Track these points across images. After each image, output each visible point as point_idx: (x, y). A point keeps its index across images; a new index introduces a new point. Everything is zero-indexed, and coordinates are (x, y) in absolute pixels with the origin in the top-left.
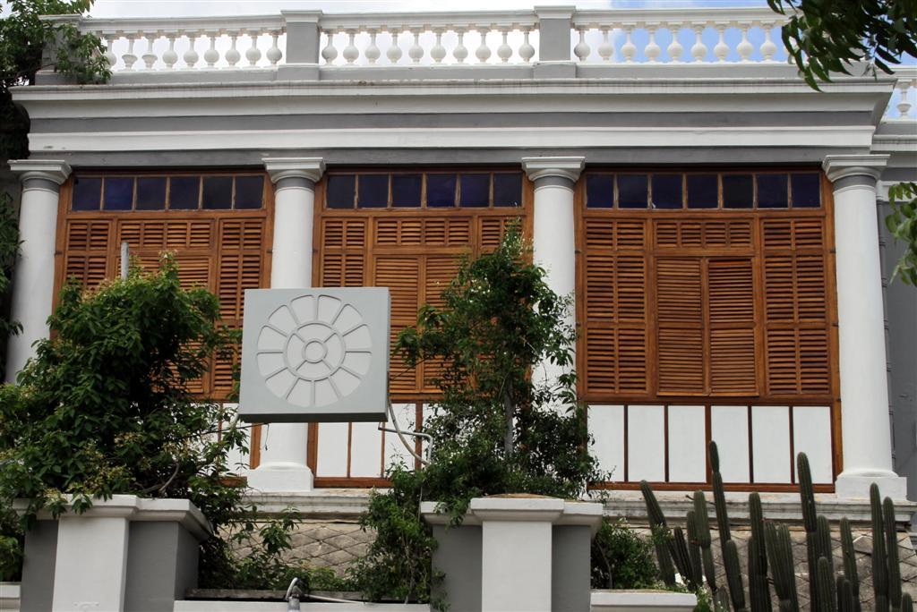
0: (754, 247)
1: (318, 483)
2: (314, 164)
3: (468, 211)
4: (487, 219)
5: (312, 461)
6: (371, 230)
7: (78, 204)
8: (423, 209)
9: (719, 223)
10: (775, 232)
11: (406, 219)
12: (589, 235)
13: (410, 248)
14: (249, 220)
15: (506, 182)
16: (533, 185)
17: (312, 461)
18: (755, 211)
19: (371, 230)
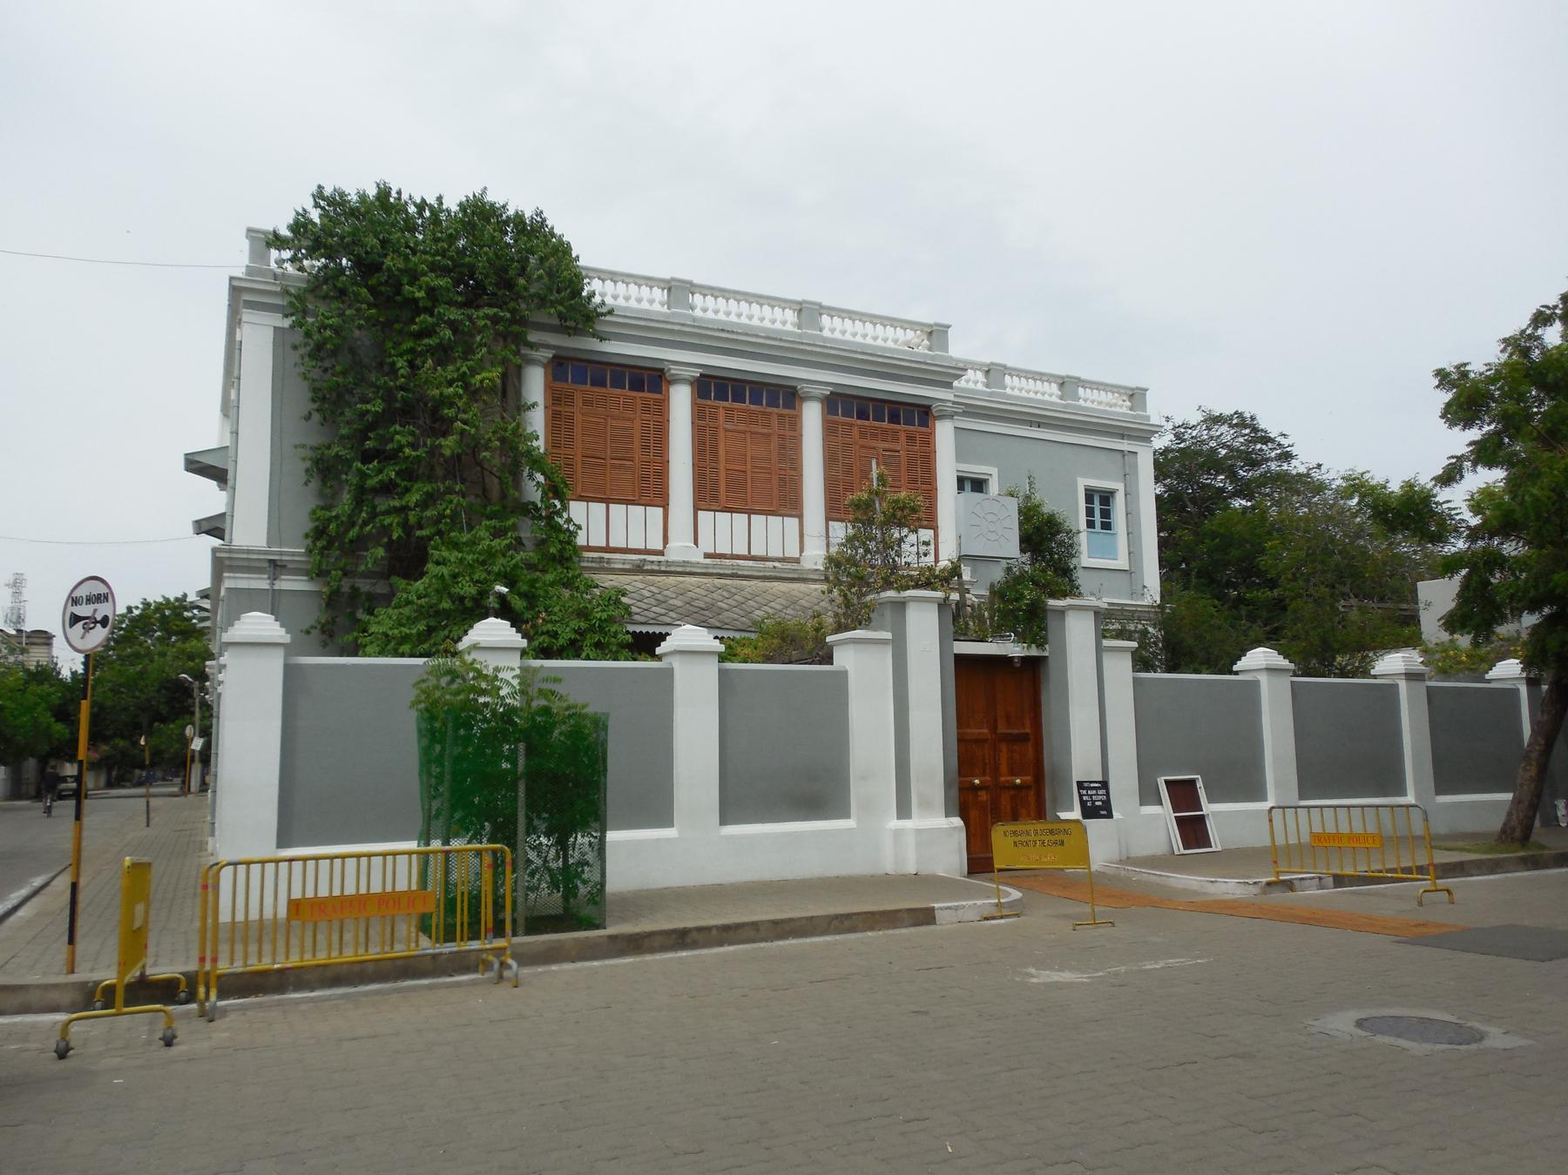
0: (901, 444)
1: (707, 556)
2: (696, 373)
3: (770, 410)
4: (780, 415)
5: (696, 543)
6: (722, 411)
7: (555, 379)
8: (747, 405)
9: (885, 431)
10: (911, 438)
11: (739, 410)
12: (829, 430)
13: (742, 427)
14: (656, 400)
15: (787, 396)
16: (803, 399)
17: (696, 543)
18: (902, 427)
19: (722, 411)
